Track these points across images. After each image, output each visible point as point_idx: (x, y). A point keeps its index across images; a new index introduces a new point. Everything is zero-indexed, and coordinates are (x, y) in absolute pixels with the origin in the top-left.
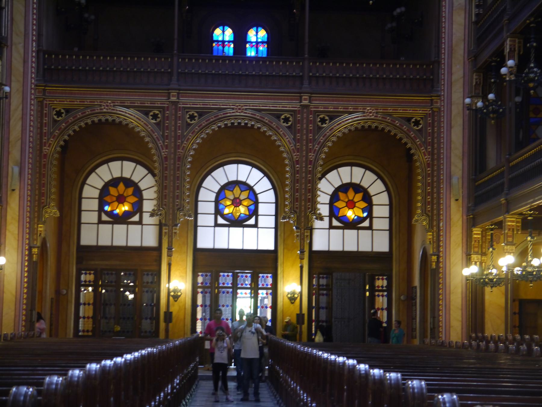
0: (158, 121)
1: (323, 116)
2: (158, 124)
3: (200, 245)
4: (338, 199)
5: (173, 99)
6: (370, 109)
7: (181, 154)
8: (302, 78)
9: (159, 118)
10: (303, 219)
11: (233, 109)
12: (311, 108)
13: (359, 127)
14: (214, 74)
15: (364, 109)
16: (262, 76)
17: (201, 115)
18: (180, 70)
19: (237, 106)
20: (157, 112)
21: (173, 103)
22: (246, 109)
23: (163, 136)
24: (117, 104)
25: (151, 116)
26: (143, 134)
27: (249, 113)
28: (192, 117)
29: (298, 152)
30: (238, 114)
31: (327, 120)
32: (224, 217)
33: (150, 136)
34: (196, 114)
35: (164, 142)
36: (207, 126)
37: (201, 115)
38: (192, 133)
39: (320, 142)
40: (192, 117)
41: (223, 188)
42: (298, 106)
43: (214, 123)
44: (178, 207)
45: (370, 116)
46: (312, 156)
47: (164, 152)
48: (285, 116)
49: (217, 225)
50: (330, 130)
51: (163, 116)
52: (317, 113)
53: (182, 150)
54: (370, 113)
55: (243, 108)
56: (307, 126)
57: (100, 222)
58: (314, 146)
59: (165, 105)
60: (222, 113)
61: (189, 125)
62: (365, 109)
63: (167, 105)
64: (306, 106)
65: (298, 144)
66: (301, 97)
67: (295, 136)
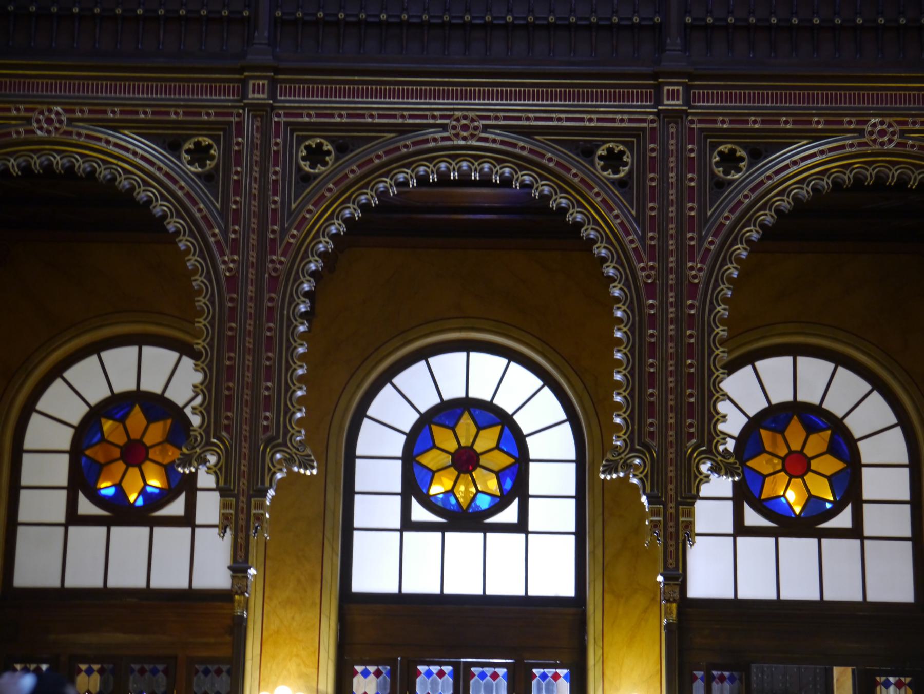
0: (208, 168)
1: (729, 146)
2: (208, 178)
3: (361, 583)
4: (760, 450)
5: (254, 97)
6: (882, 123)
7: (278, 266)
8: (658, 30)
9: (212, 158)
10: (671, 471)
11: (444, 127)
12: (692, 122)
13: (847, 177)
14: (388, 24)
15: (858, 122)
16: (535, 26)
17: (342, 149)
18: (279, 14)
19: (458, 120)
20: (206, 141)
21: (257, 109)
22: (486, 128)
23: (224, 212)
24: (79, 115)
25: (188, 151)
26: (159, 208)
27: (494, 141)
28: (316, 155)
29: (652, 259)
30: (462, 143)
31: (742, 159)
32: (428, 503)
33: (182, 210)
34: (328, 147)
35: (225, 233)
36: (365, 181)
37: (342, 149)
38: (315, 205)
39: (722, 225)
40: (316, 155)
41: (427, 420)
42: (651, 117)
43: (385, 170)
44: (269, 434)
45: (882, 144)
46: (696, 270)
47: (226, 264)
48: (610, 150)
49: (408, 525)
50: (753, 190)
51: (227, 151)
52: (714, 136)
53: (284, 254)
54: (882, 133)
55: (476, 124)
56: (680, 178)
57: (73, 518)
58: (701, 239)
59: (232, 119)
60: (408, 142)
61: (306, 179)
62: (865, 122)
63: (237, 119)
64: (675, 116)
65: (651, 234)
66: (658, 88)
67: (641, 209)
